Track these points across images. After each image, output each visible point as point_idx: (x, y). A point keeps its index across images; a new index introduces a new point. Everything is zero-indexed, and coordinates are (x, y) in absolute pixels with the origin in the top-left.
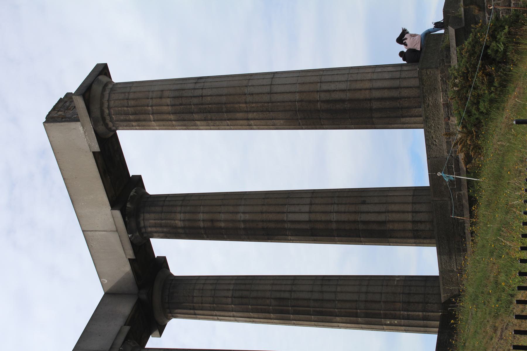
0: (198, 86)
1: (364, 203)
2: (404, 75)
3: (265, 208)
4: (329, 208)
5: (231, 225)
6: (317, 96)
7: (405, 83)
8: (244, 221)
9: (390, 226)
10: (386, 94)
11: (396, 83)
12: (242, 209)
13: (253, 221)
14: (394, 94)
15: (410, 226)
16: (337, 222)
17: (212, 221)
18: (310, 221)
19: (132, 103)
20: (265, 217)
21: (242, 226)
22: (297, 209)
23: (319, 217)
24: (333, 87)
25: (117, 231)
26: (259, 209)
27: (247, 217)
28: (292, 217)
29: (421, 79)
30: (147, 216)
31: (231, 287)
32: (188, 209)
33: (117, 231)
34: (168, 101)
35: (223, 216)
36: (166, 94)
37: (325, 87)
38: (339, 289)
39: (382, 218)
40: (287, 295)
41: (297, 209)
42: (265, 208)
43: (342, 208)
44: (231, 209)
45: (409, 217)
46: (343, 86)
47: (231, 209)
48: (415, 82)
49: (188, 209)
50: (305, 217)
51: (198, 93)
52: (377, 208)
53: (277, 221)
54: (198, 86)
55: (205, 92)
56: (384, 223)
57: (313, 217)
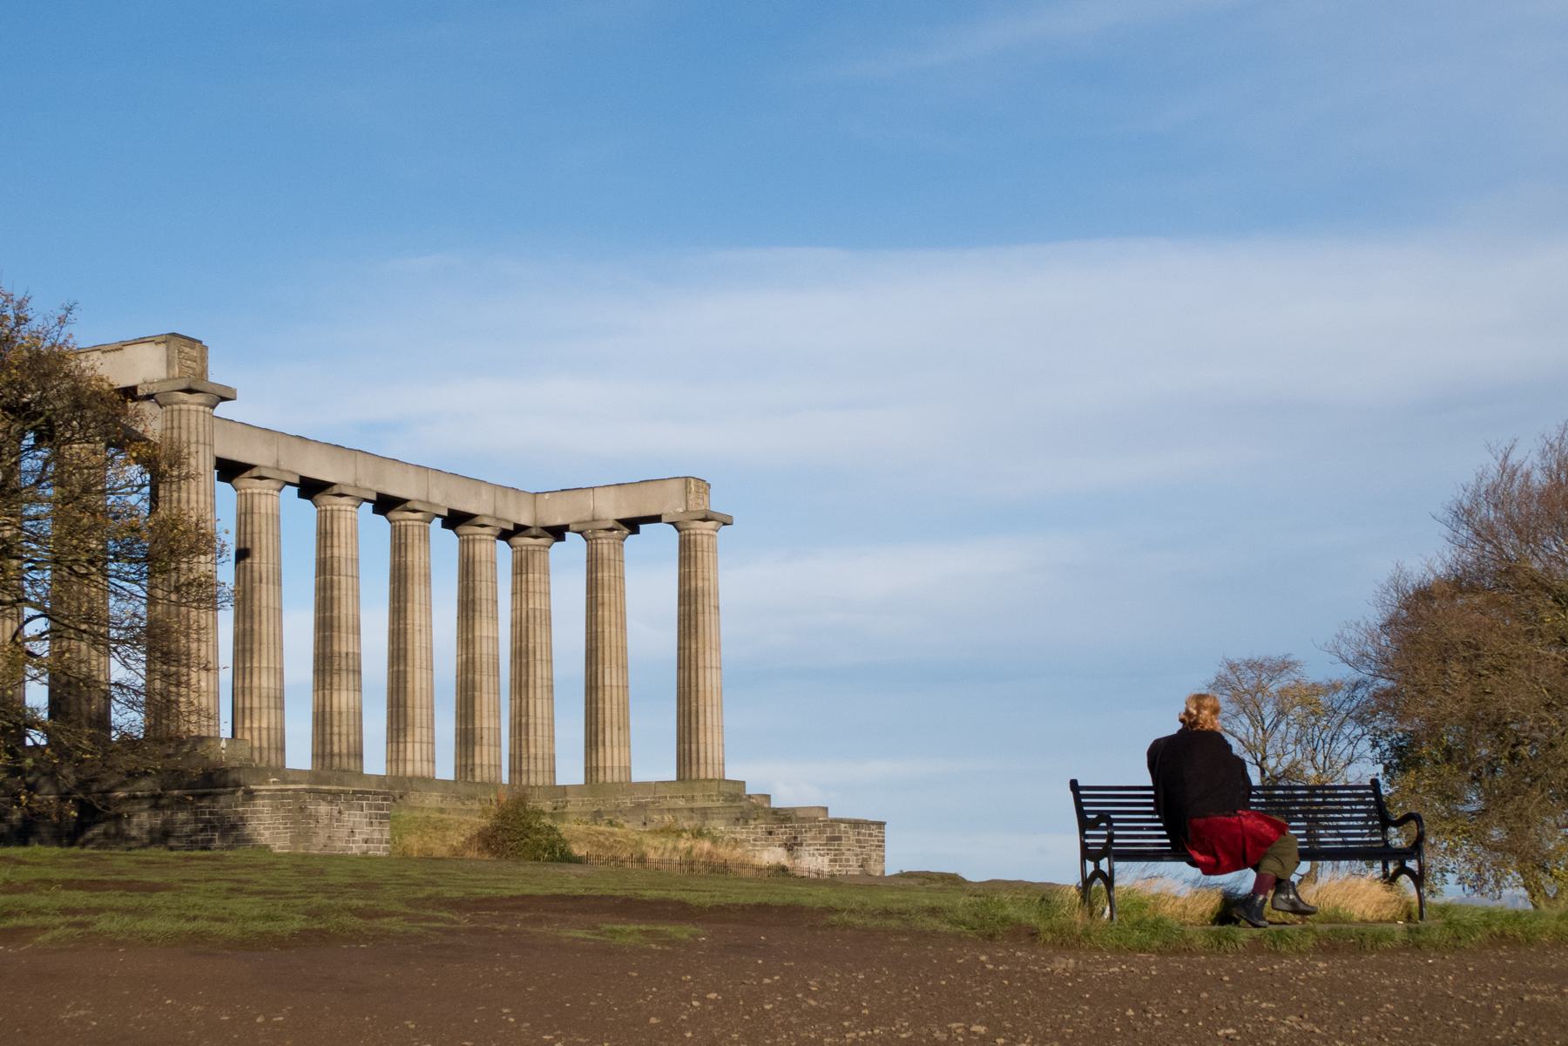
0: (712, 608)
1: (619, 729)
2: (716, 766)
3: (614, 649)
4: (615, 702)
5: (600, 619)
7: (709, 768)
8: (603, 631)
9: (601, 749)
10: (702, 755)
11: (710, 761)
12: (613, 629)
13: (603, 639)
14: (702, 760)
15: (601, 764)
16: (604, 708)
17: (603, 604)
18: (604, 686)
19: (699, 554)
20: (607, 649)
21: (599, 630)
22: (614, 675)
24: (708, 714)
25: (594, 520)
26: (614, 644)
27: (607, 634)
28: (607, 671)
29: (711, 780)
30: (606, 547)
31: (543, 607)
32: (613, 583)
33: (594, 520)
34: (700, 584)
35: (606, 613)
36: (706, 584)
37: (708, 709)
38: (545, 701)
39: (608, 743)
40: (538, 657)
41: (614, 675)
42: (614, 649)
43: (615, 712)
44: (613, 620)
45: (608, 764)
46: (709, 723)
47: (613, 620)
48: (710, 776)
49: (613, 583)
50: (607, 682)
51: (707, 610)
52: (615, 739)
53: (603, 659)
54: (712, 608)
55: (707, 615)
56: (604, 745)
57: (607, 689)
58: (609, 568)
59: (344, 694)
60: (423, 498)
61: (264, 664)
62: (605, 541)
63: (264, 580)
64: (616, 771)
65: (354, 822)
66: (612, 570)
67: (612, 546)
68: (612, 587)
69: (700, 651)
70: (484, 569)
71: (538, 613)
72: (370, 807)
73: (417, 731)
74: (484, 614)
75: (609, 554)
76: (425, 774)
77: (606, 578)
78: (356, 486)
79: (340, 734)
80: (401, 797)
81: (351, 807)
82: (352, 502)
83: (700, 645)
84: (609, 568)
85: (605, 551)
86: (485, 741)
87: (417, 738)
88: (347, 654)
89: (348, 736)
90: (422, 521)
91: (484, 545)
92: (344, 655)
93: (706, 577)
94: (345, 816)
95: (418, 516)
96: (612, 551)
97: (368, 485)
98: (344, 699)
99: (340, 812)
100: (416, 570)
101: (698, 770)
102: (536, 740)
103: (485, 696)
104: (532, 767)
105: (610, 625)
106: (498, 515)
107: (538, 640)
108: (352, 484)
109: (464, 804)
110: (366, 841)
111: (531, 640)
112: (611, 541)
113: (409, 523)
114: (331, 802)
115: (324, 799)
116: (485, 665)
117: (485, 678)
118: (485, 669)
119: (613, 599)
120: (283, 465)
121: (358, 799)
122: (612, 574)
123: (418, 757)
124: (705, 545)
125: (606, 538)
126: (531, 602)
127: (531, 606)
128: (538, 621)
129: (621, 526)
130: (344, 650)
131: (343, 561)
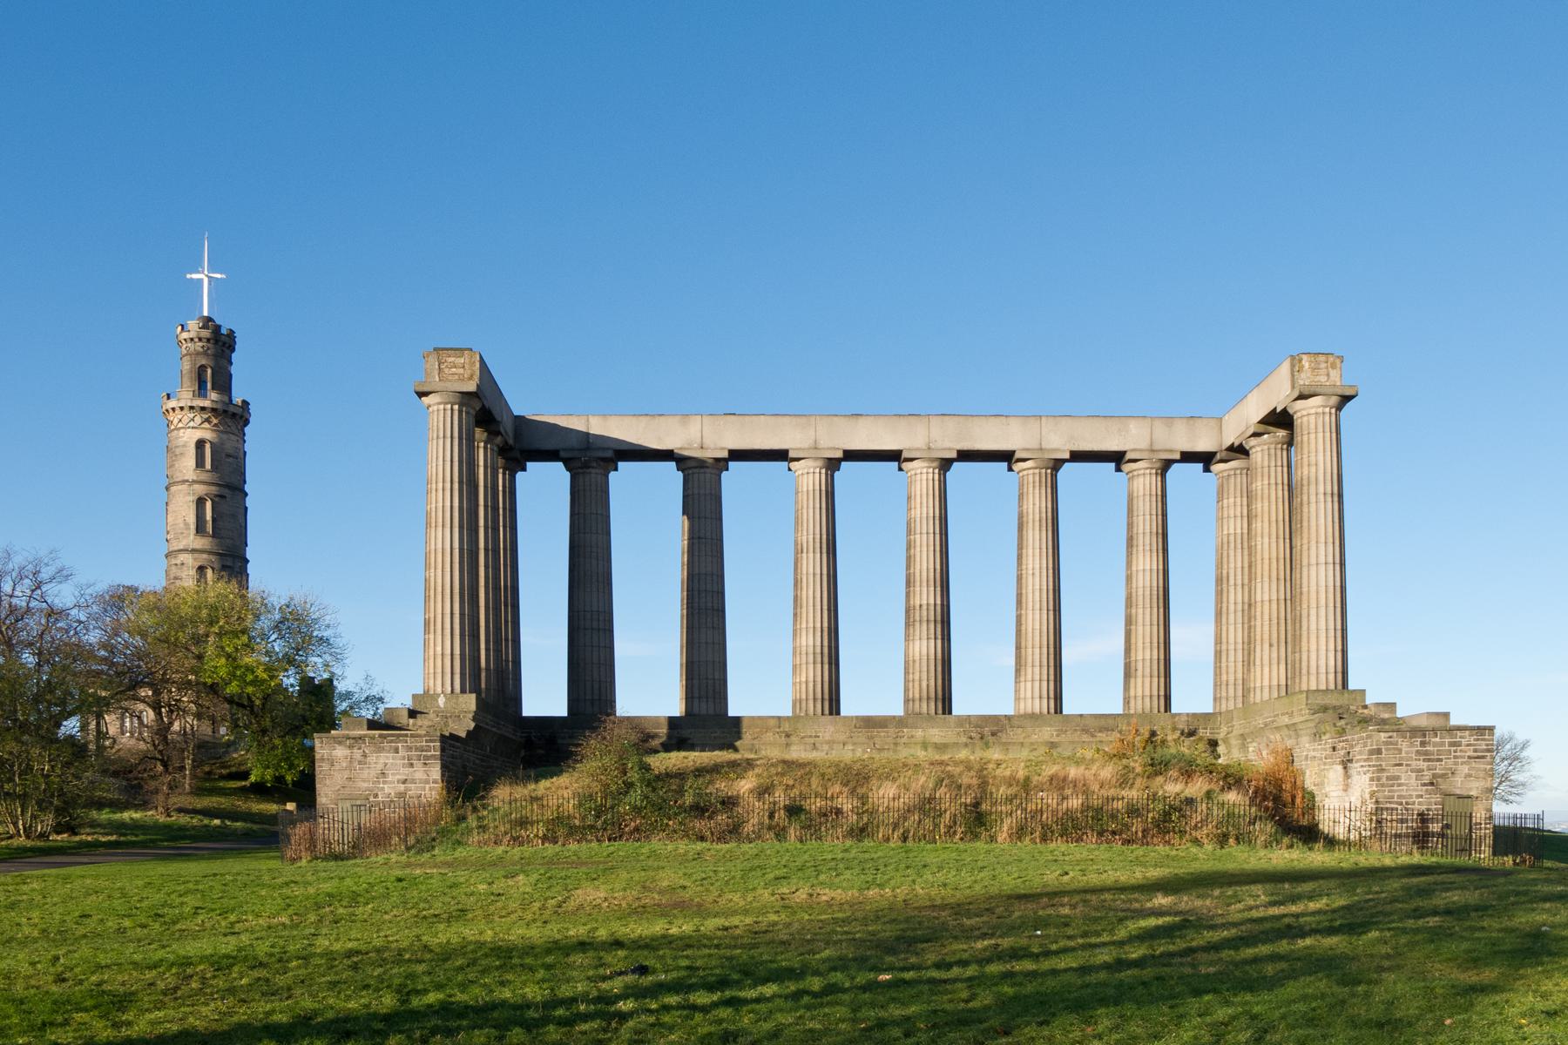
6: (1305, 606)
20: (1259, 562)
23: (1259, 609)
27: (1259, 547)
28: (1259, 585)
30: (1259, 455)
32: (1266, 491)
40: (1232, 582)
51: (1313, 499)
57: (1259, 605)
58: (1262, 476)
59: (917, 643)
60: (1035, 445)
61: (804, 626)
62: (1258, 449)
63: (805, 550)
64: (1266, 690)
65: (386, 764)
66: (1266, 478)
67: (1266, 452)
68: (1266, 495)
69: (1305, 547)
70: (1141, 504)
71: (1232, 538)
72: (409, 749)
73: (1029, 670)
74: (1141, 548)
75: (1263, 461)
76: (1037, 710)
77: (1259, 488)
78: (1041, 449)
79: (913, 680)
80: (993, 734)
81: (381, 750)
82: (926, 464)
83: (1305, 541)
84: (1262, 476)
85: (1259, 459)
86: (1140, 673)
87: (1029, 677)
88: (921, 606)
89: (920, 680)
90: (1036, 468)
91: (1141, 479)
92: (918, 608)
93: (1313, 462)
94: (372, 758)
95: (1029, 464)
96: (1266, 457)
97: (948, 444)
98: (917, 649)
99: (365, 756)
100: (1031, 517)
101: (1300, 683)
102: (1227, 666)
103: (1140, 629)
104: (1224, 694)
105: (1262, 537)
106: (1156, 447)
107: (1232, 565)
108: (924, 447)
109: (1093, 736)
110: (405, 782)
111: (1225, 567)
112: (1266, 447)
113: (1025, 473)
114: (351, 747)
115: (340, 743)
116: (1141, 598)
117: (1140, 611)
118: (1141, 603)
119: (1266, 509)
120: (823, 443)
121: (391, 742)
122: (1266, 482)
123: (1029, 694)
124: (1312, 426)
125: (1259, 445)
126: (1225, 528)
127: (1225, 532)
128: (1232, 545)
129: (1271, 428)
130: (918, 603)
131: (918, 520)
